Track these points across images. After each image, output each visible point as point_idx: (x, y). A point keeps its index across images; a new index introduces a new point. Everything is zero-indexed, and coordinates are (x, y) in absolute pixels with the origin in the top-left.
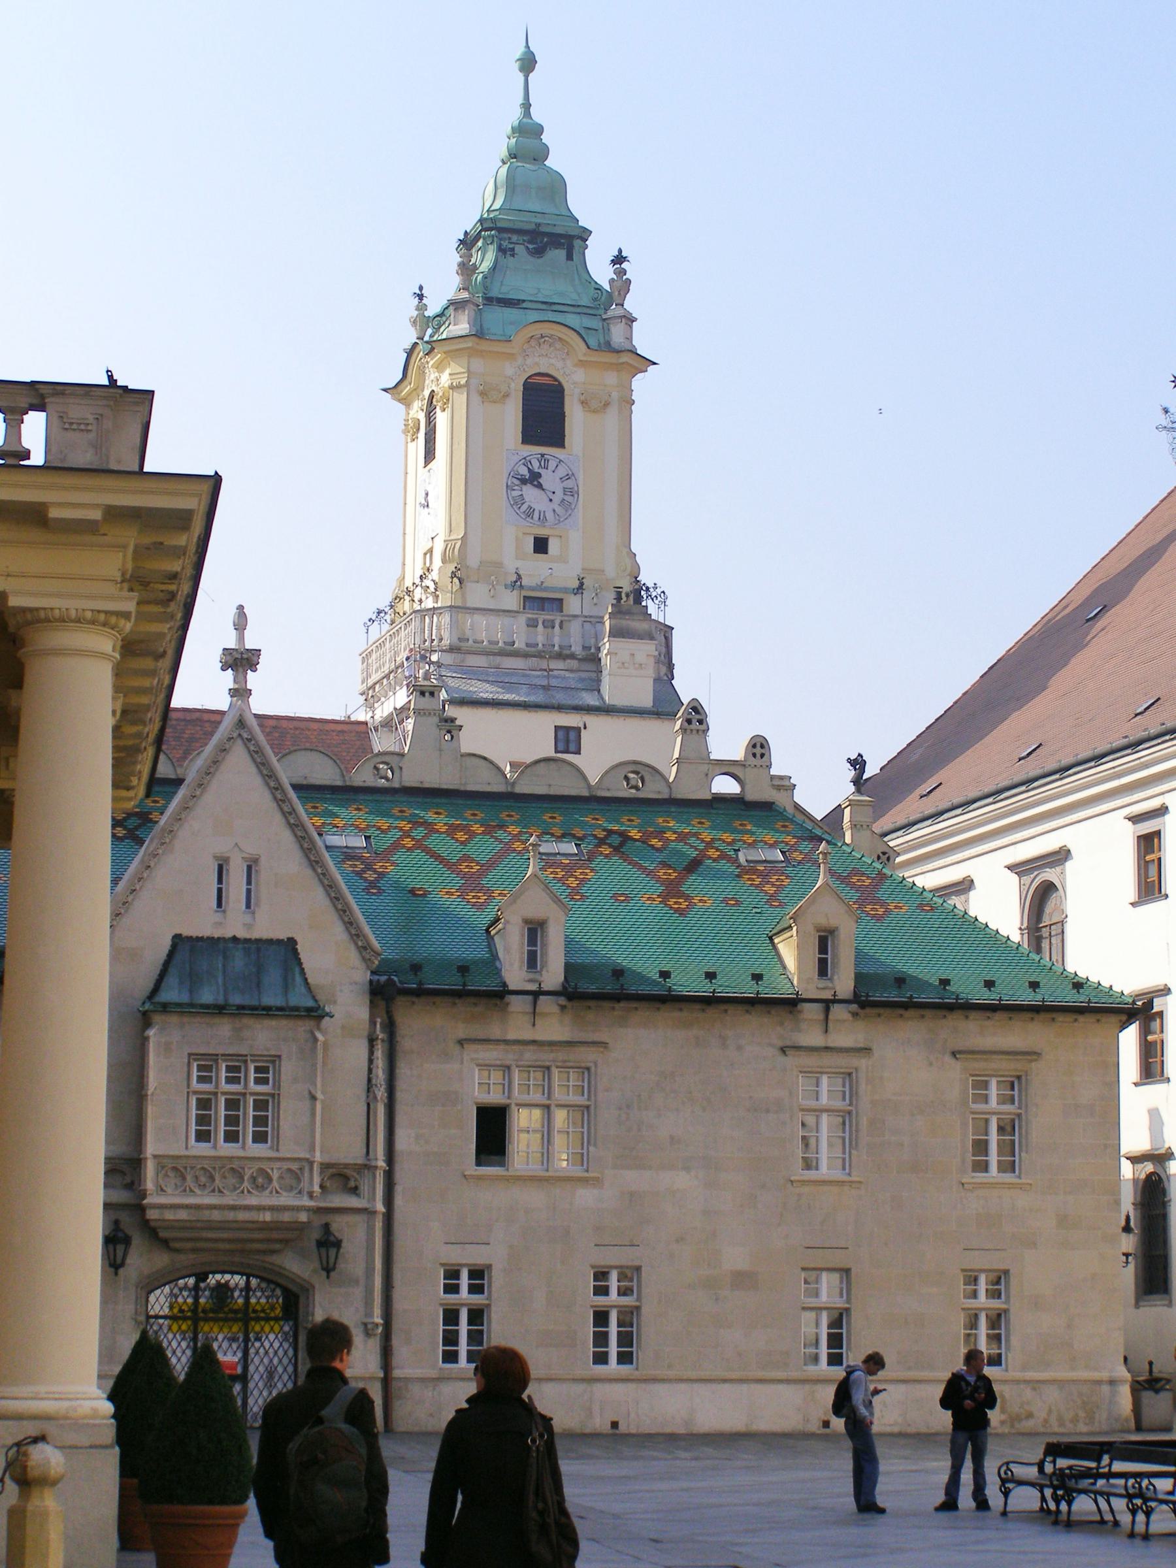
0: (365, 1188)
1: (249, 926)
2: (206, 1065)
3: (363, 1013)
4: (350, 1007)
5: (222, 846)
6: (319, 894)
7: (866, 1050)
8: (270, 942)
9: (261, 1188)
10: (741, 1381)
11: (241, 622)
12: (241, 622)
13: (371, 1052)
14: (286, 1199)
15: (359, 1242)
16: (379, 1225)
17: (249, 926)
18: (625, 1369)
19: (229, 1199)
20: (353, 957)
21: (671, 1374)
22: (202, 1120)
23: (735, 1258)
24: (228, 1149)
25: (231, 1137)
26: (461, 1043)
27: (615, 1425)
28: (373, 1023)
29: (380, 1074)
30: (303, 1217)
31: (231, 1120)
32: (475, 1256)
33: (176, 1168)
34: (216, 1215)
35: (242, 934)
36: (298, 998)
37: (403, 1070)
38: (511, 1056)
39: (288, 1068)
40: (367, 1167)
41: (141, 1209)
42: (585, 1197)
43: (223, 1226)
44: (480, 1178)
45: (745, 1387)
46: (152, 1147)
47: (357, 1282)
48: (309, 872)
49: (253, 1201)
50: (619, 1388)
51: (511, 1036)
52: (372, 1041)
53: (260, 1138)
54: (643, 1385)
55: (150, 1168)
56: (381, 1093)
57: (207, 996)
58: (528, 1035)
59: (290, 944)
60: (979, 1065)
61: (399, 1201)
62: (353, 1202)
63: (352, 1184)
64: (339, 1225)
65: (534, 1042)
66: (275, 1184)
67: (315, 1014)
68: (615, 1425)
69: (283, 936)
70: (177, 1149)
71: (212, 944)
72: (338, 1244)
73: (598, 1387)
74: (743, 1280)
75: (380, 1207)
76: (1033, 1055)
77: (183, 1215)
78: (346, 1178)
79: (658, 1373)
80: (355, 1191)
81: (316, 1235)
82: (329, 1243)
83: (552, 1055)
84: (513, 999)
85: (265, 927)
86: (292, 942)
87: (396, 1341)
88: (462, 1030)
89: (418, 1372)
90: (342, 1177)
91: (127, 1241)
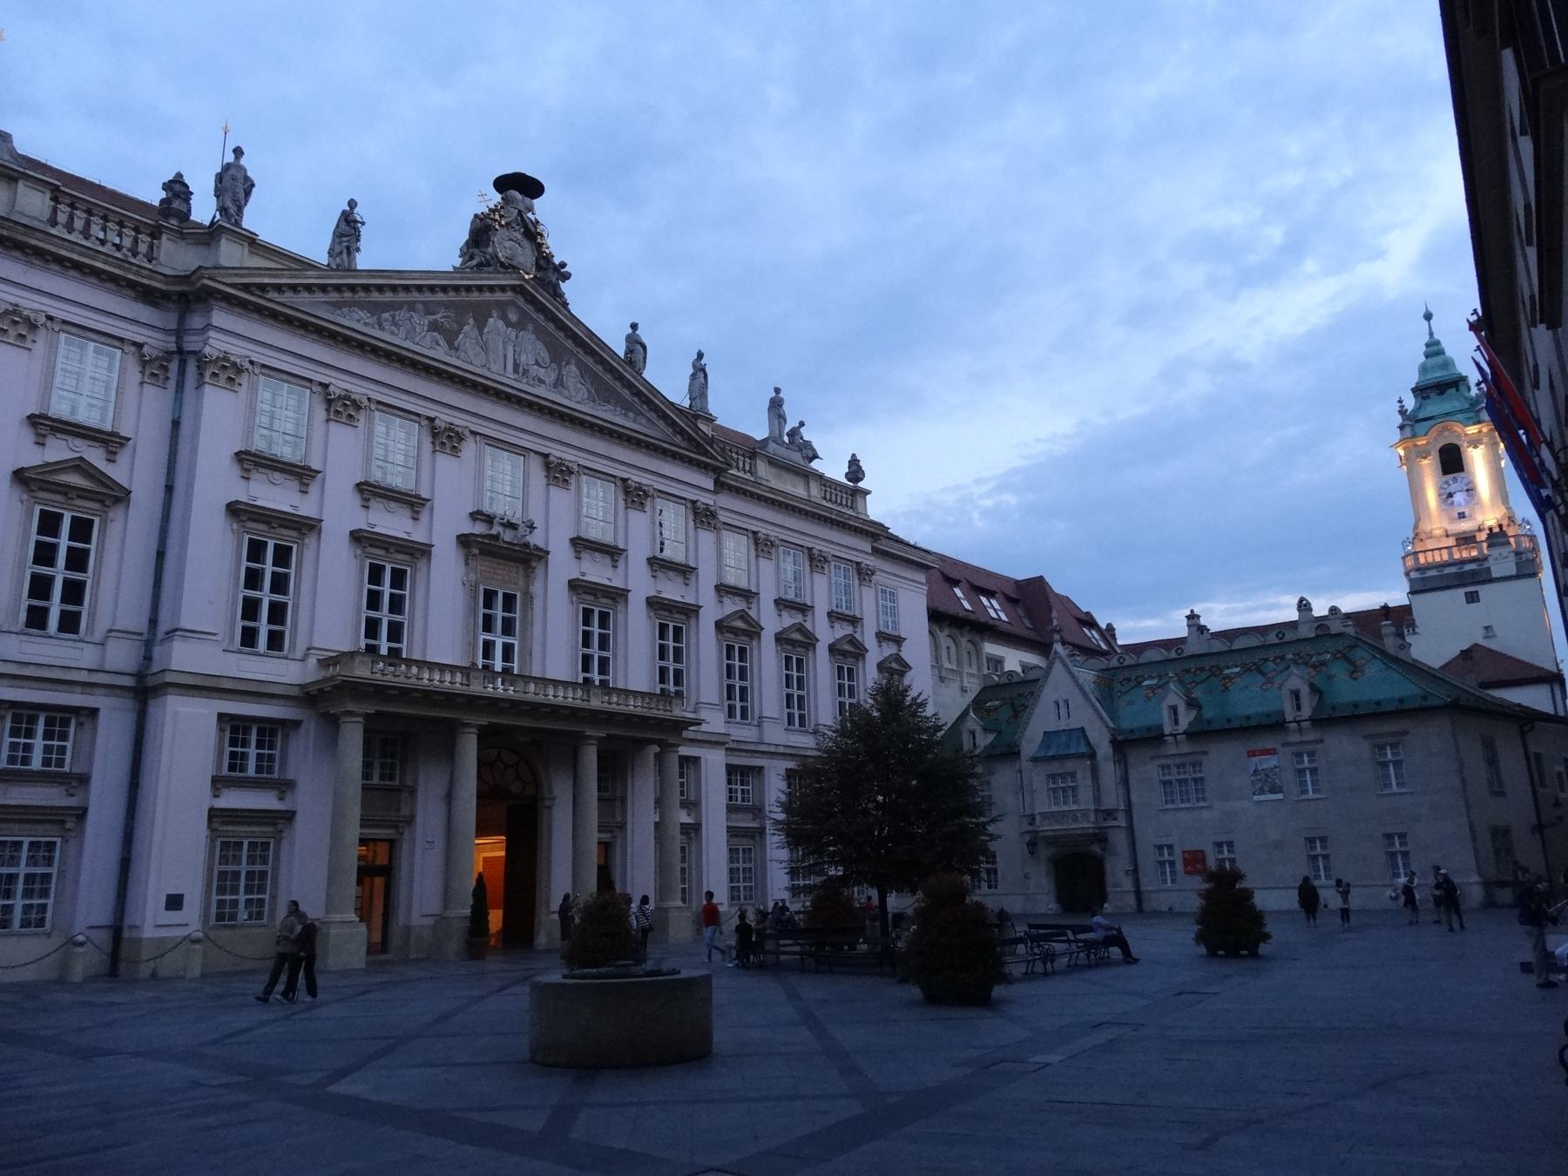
5: (1055, 697)
6: (1091, 711)
15: (1119, 840)
20: (1105, 731)
24: (1066, 808)
25: (1065, 803)
26: (1153, 758)
32: (1165, 841)
33: (1044, 816)
37: (1132, 772)
42: (1205, 813)
59: (1082, 730)
62: (1115, 823)
71: (1056, 733)
85: (1074, 723)
86: (1082, 730)
87: (1141, 876)
90: (1110, 814)
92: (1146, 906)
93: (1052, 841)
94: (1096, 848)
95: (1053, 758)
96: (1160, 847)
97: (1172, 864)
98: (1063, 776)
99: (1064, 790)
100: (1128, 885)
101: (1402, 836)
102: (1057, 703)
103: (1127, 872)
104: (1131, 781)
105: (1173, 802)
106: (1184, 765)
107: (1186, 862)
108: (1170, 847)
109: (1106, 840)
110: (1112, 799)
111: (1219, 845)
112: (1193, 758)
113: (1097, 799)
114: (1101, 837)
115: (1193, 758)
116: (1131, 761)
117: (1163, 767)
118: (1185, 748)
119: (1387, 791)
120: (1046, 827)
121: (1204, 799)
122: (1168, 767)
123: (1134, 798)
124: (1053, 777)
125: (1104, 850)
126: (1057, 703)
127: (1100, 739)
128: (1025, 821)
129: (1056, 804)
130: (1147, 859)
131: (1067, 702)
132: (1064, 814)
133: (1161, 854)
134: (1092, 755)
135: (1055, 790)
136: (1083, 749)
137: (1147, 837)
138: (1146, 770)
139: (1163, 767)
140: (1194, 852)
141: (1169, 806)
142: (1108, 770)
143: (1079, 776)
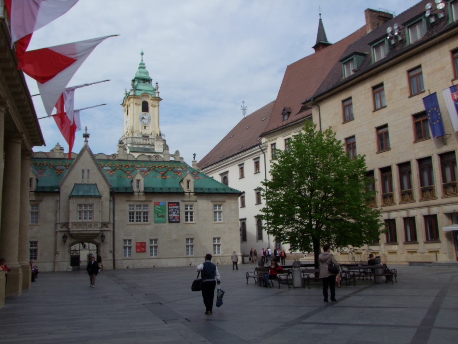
1: (88, 181)
2: (80, 205)
4: (106, 194)
5: (83, 168)
6: (100, 176)
7: (196, 201)
8: (92, 184)
9: (90, 227)
11: (86, 129)
12: (86, 129)
14: (95, 229)
15: (109, 236)
16: (112, 233)
17: (88, 181)
18: (156, 257)
19: (85, 229)
20: (106, 186)
22: (80, 215)
23: (174, 237)
25: (85, 219)
26: (126, 201)
27: (154, 266)
29: (112, 207)
30: (98, 232)
31: (85, 215)
33: (75, 224)
34: (83, 232)
35: (87, 183)
36: (97, 194)
39: (95, 206)
41: (69, 231)
42: (148, 227)
43: (83, 234)
44: (130, 224)
46: (71, 220)
48: (99, 172)
49: (89, 229)
51: (135, 199)
52: (110, 201)
53: (90, 219)
55: (70, 225)
56: (112, 210)
57: (81, 194)
59: (96, 184)
60: (215, 203)
61: (115, 229)
64: (105, 233)
67: (100, 197)
68: (154, 266)
69: (94, 183)
70: (75, 221)
72: (104, 237)
73: (151, 260)
74: (176, 240)
75: (112, 230)
76: (225, 201)
77: (76, 232)
80: (107, 227)
81: (101, 235)
82: (103, 237)
84: (135, 193)
85: (91, 181)
89: (120, 259)
90: (105, 224)
91: (66, 237)
92: (116, 266)
93: (72, 236)
95: (82, 196)
96: (125, 241)
97: (130, 248)
98: (86, 205)
99: (85, 212)
100: (110, 257)
102: (83, 171)
105: (133, 221)
106: (140, 206)
107: (137, 247)
108: (130, 241)
110: (106, 219)
111: (151, 240)
112: (145, 203)
115: (145, 203)
117: (130, 206)
118: (143, 198)
119: (216, 222)
120: (73, 229)
121: (147, 221)
122: (133, 205)
123: (116, 218)
124: (80, 205)
126: (83, 171)
127: (104, 190)
128: (59, 226)
129: (80, 219)
130: (120, 245)
131: (88, 171)
132: (85, 223)
135: (80, 212)
137: (121, 235)
138: (124, 207)
139: (130, 206)
140: (141, 243)
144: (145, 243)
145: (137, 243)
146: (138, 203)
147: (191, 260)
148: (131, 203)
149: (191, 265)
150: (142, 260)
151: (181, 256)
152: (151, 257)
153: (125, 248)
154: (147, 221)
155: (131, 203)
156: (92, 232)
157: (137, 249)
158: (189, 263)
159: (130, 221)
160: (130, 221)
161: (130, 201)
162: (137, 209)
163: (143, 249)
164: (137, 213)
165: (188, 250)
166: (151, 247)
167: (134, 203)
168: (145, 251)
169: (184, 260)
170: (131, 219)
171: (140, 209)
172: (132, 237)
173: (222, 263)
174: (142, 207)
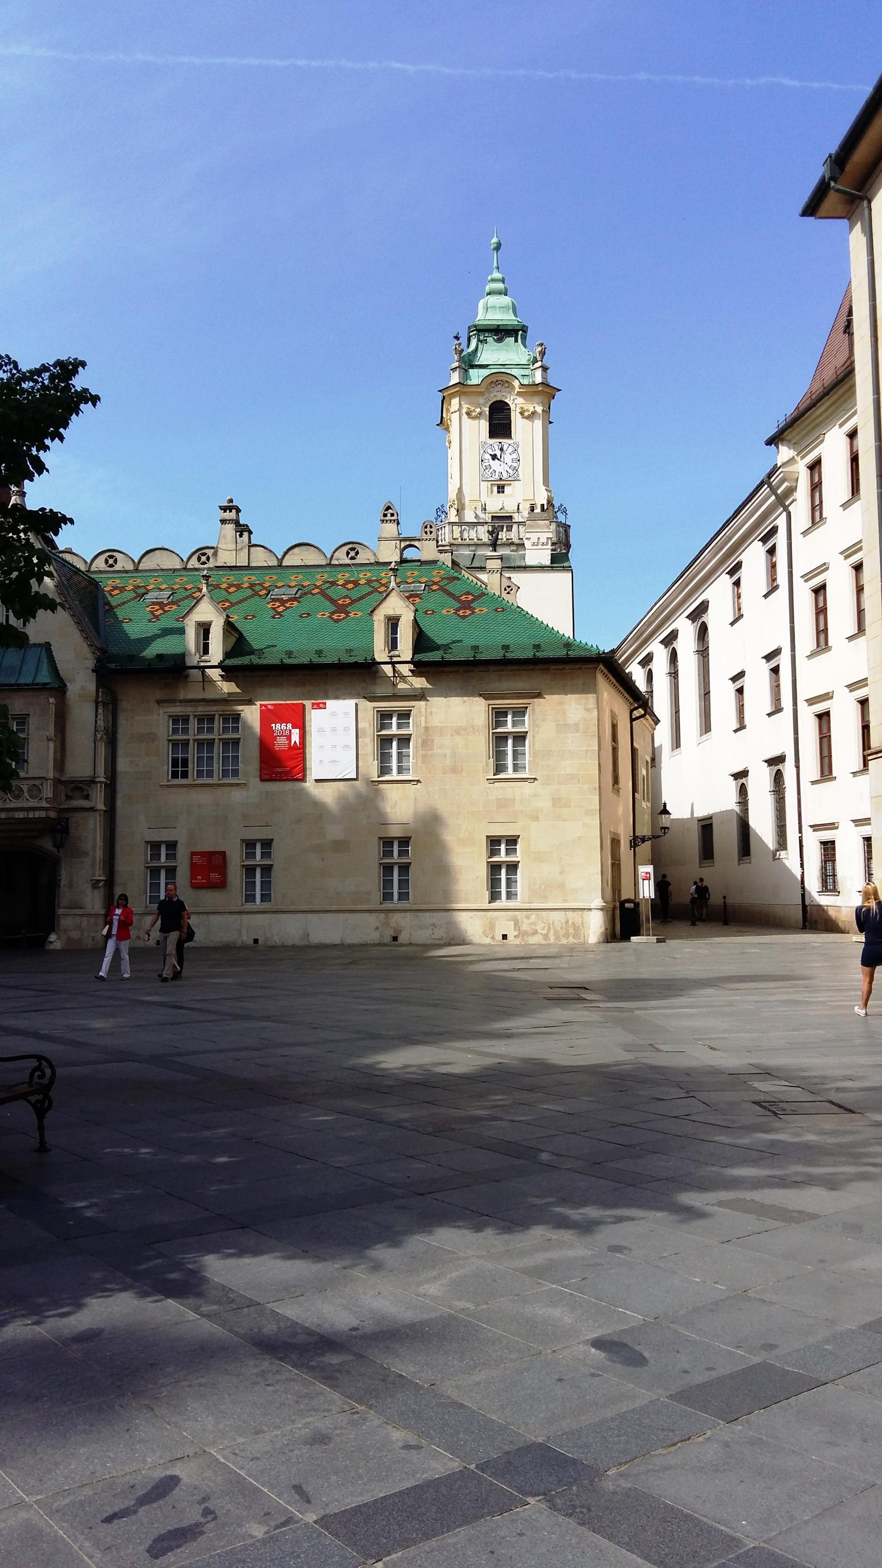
0: (93, 795)
3: (92, 687)
10: (339, 911)
13: (97, 711)
14: (33, 803)
15: (90, 832)
18: (266, 906)
21: (293, 908)
26: (159, 702)
28: (97, 692)
38: (189, 709)
40: (92, 781)
42: (237, 796)
45: (341, 915)
47: (87, 854)
49: (12, 805)
50: (260, 916)
51: (190, 696)
52: (97, 703)
54: (274, 915)
58: (200, 696)
61: (119, 803)
62: (85, 803)
63: (85, 793)
65: (203, 700)
66: (26, 794)
74: (340, 846)
75: (101, 806)
78: (83, 790)
79: (285, 908)
80: (87, 797)
83: (215, 708)
88: (159, 695)
90: (80, 787)
94: (47, 844)
96: (155, 846)
97: (171, 872)
101: (512, 841)
103: (95, 885)
104: (120, 737)
105: (185, 775)
107: (195, 869)
108: (172, 846)
109: (66, 830)
111: (250, 845)
113: (60, 764)
114: (59, 828)
116: (125, 704)
121: (235, 773)
122: (186, 719)
123: (122, 765)
125: (59, 846)
133: (156, 856)
134: (59, 688)
136: (44, 677)
137: (137, 827)
138: (149, 723)
139: (175, 720)
141: (180, 781)
142: (84, 715)
143: (33, 722)
144: (223, 854)
145: (193, 854)
146: (201, 709)
147: (397, 919)
148: (177, 710)
149: (395, 939)
150: (214, 919)
151: (359, 907)
152: (249, 906)
153: (155, 872)
154: (235, 773)
155: (177, 710)
156: (21, 815)
157: (193, 876)
158: (389, 934)
159: (175, 775)
160: (175, 775)
161: (171, 702)
162: (200, 730)
163: (215, 876)
164: (200, 743)
165: (388, 883)
166: (250, 871)
167: (189, 710)
168: (221, 885)
169: (372, 920)
170: (179, 768)
171: (211, 730)
172: (179, 834)
173: (521, 934)
174: (218, 724)
